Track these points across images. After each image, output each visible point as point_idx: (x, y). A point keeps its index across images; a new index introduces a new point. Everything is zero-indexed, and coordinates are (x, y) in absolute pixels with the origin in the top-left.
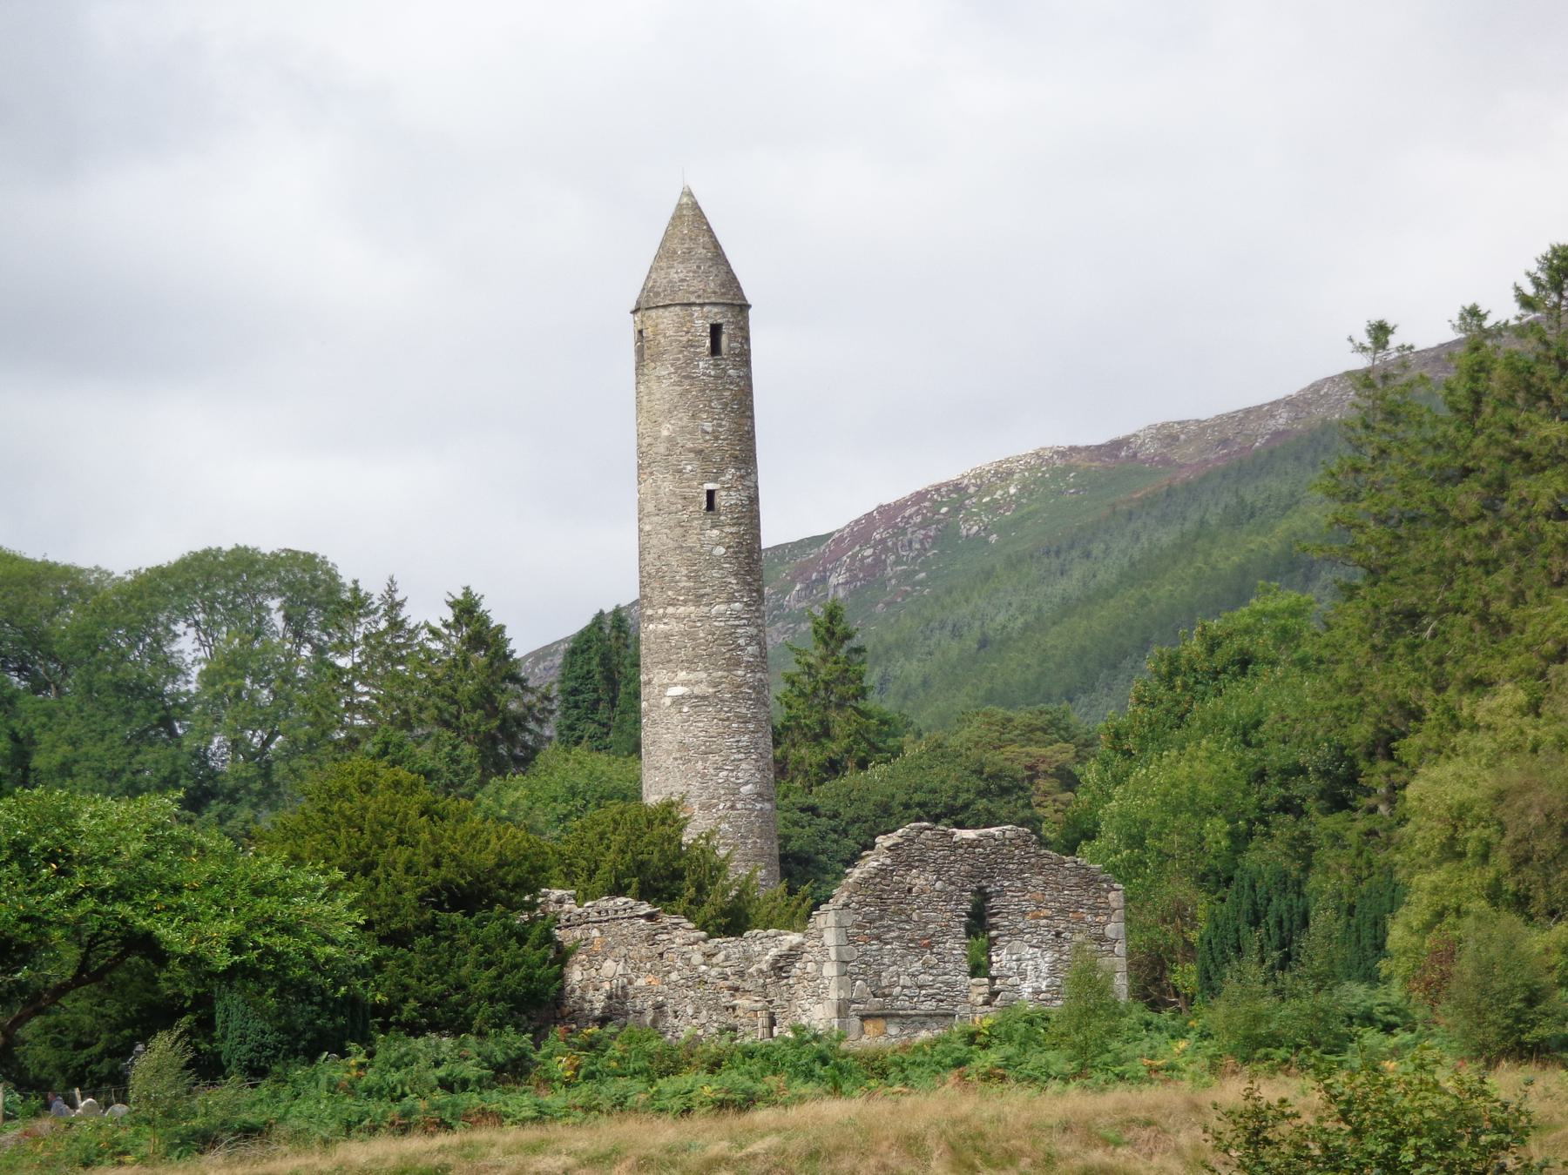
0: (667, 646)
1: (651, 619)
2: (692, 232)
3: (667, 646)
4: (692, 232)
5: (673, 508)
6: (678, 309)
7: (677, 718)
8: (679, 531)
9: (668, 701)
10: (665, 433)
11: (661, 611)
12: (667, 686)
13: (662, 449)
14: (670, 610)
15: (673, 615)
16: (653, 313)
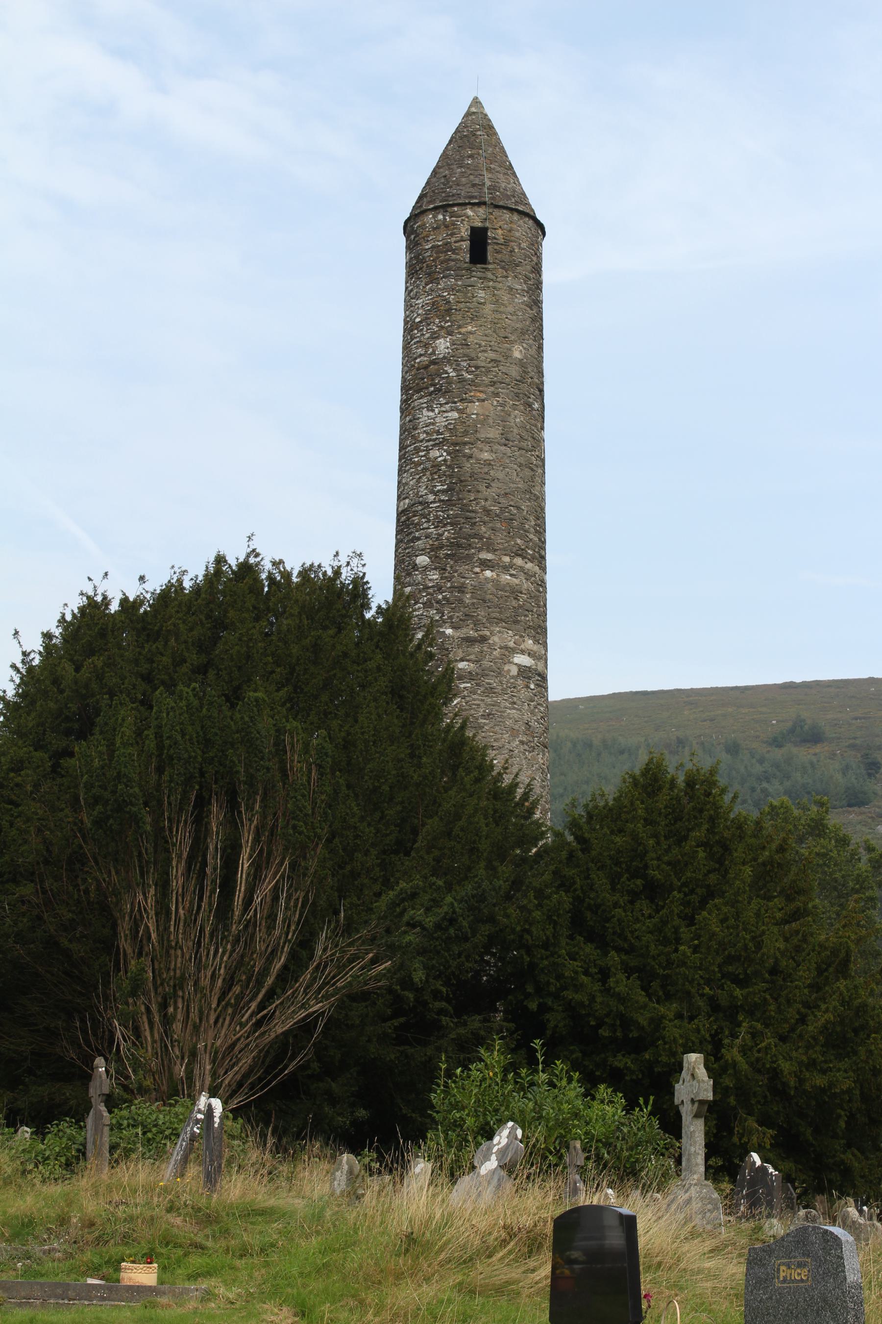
0: (514, 603)
1: (486, 564)
2: (474, 141)
3: (514, 603)
4: (474, 141)
5: (524, 444)
6: (531, 222)
7: (524, 694)
8: (528, 473)
9: (514, 671)
10: (517, 354)
11: (507, 559)
12: (513, 651)
13: (514, 372)
14: (519, 561)
15: (522, 569)
16: (507, 215)
